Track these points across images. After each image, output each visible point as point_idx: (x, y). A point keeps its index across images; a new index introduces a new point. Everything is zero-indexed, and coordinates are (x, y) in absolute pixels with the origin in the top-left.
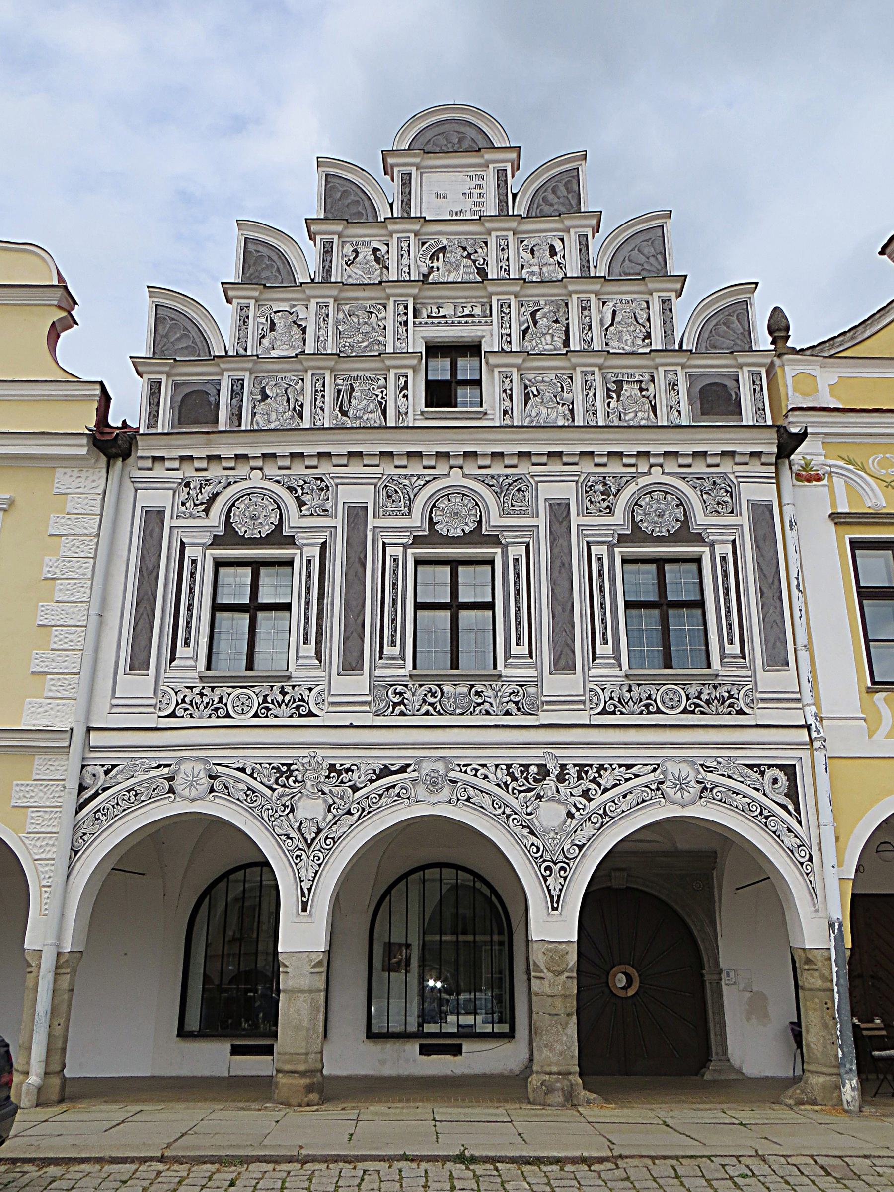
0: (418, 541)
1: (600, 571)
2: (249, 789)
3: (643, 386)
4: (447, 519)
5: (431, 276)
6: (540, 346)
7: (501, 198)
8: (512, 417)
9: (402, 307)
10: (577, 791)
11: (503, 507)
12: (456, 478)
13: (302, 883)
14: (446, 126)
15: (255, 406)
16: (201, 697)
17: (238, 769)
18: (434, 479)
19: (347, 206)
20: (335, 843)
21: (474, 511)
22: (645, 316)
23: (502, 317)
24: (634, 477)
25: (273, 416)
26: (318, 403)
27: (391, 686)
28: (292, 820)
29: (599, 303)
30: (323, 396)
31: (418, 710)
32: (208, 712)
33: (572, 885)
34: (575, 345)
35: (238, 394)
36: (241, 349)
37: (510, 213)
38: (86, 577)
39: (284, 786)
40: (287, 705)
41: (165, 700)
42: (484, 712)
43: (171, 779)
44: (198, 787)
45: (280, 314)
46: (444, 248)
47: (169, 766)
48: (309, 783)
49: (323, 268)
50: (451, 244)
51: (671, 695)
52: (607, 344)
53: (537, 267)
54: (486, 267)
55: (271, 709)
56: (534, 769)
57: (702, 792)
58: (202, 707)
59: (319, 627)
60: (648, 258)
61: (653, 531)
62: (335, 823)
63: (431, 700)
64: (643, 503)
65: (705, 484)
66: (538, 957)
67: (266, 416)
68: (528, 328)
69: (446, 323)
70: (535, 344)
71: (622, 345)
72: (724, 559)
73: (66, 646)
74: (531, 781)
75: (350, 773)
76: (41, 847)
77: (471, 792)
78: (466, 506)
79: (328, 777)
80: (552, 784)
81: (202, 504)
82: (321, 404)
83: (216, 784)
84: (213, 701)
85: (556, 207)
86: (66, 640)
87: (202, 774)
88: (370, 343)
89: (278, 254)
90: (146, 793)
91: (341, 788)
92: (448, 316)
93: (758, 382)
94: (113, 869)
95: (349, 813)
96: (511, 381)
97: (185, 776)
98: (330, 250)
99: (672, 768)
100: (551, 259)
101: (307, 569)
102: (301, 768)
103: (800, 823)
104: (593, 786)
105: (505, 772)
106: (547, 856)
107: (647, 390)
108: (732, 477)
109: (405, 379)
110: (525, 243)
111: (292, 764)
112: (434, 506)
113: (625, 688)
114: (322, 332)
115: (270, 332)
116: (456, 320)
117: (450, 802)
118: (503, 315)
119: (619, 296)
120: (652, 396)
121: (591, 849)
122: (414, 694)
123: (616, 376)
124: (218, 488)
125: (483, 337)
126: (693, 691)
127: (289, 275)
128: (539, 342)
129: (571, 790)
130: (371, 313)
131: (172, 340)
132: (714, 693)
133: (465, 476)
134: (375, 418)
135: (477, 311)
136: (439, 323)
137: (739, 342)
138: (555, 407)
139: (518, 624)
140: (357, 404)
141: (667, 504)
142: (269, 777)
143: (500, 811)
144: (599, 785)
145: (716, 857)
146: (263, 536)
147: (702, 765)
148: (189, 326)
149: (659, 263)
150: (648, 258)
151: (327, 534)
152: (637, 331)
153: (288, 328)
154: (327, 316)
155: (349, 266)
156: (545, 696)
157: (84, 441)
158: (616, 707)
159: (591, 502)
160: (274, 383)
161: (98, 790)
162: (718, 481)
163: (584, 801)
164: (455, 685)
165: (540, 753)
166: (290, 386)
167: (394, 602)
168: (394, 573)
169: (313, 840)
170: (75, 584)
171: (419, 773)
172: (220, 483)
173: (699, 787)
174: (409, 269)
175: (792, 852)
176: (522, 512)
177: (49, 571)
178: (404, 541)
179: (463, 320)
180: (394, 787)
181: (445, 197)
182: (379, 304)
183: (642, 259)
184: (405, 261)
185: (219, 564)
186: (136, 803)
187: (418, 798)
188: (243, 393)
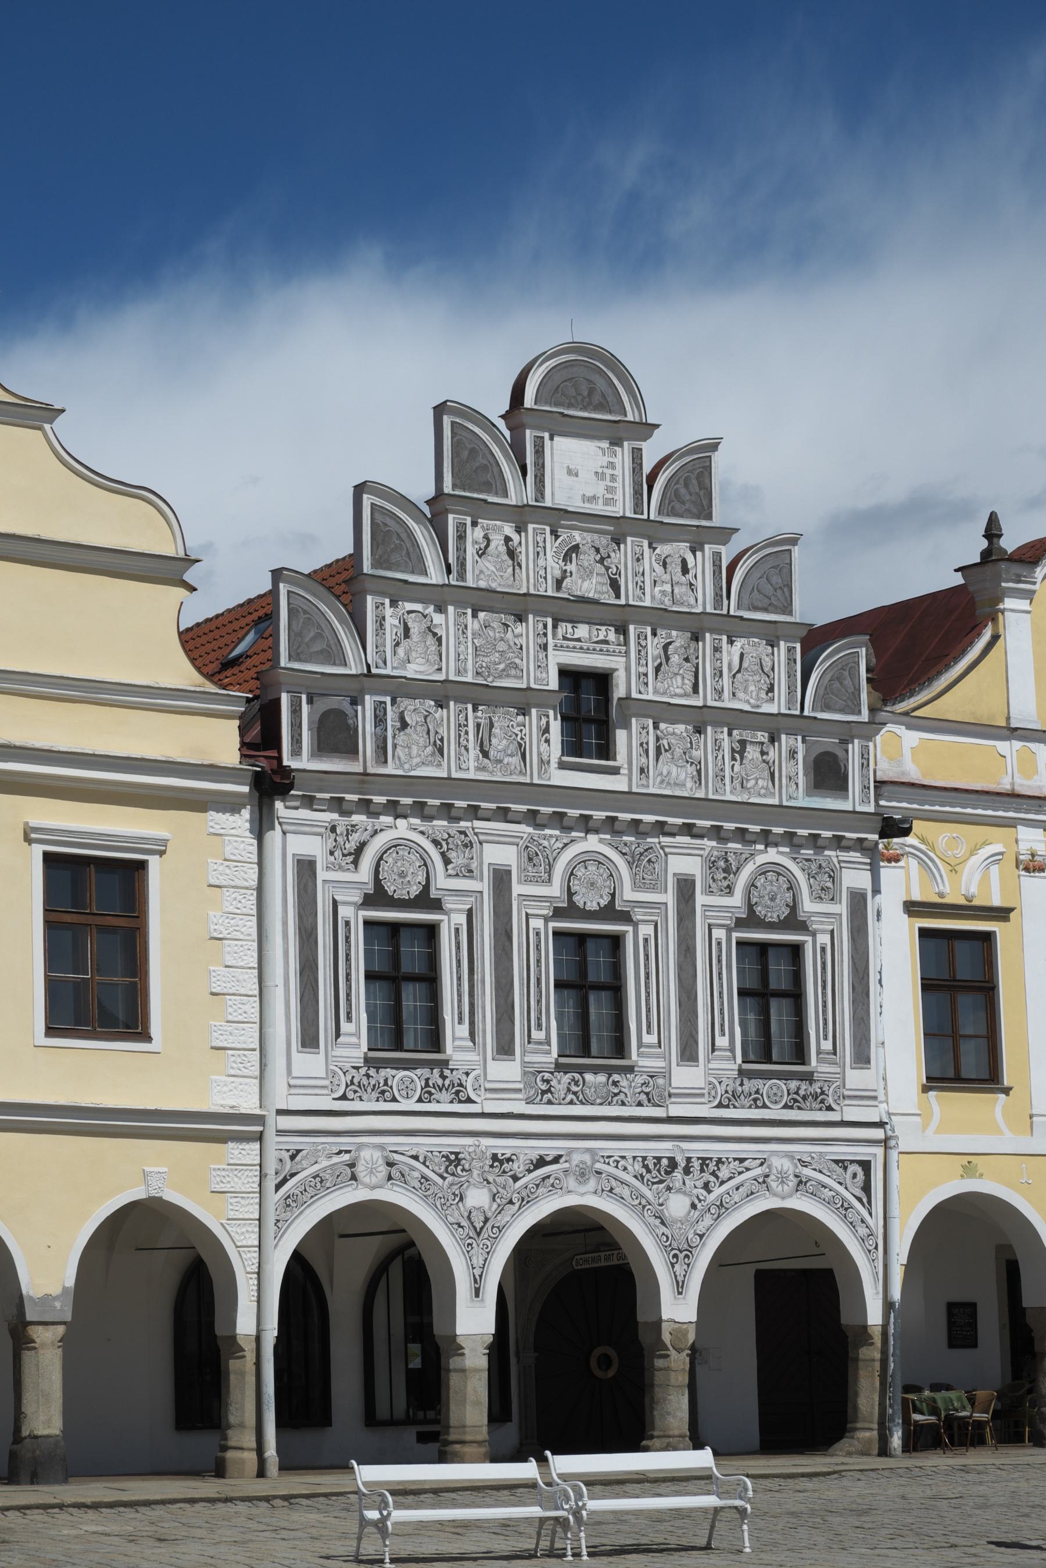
0: (558, 913)
2: (423, 1177)
4: (584, 890)
5: (564, 584)
6: (671, 688)
8: (648, 777)
9: (541, 626)
10: (700, 1184)
13: (475, 1271)
15: (395, 735)
16: (368, 1079)
18: (572, 841)
20: (500, 1231)
21: (608, 882)
22: (770, 664)
23: (640, 651)
24: (752, 855)
25: (415, 750)
27: (540, 1072)
28: (462, 1209)
30: (467, 733)
31: (564, 1099)
32: (375, 1095)
33: (694, 1270)
35: (381, 720)
36: (381, 662)
38: (249, 938)
39: (453, 1174)
40: (447, 1090)
42: (620, 1102)
43: (352, 1165)
44: (378, 1174)
45: (414, 614)
47: (348, 1152)
48: (475, 1172)
49: (458, 558)
50: (584, 542)
52: (734, 694)
53: (669, 586)
54: (619, 579)
55: (433, 1094)
56: (665, 1162)
57: (798, 1185)
58: (369, 1090)
59: (472, 1005)
61: (766, 915)
62: (500, 1213)
63: (574, 1088)
64: (758, 884)
66: (666, 1337)
67: (407, 750)
68: (660, 665)
70: (666, 686)
71: (748, 698)
72: (823, 949)
73: (240, 1018)
74: (662, 1173)
75: (511, 1163)
76: (243, 1233)
77: (614, 1183)
78: (602, 876)
79: (492, 1166)
81: (350, 854)
82: (465, 742)
84: (379, 1083)
85: (687, 506)
86: (240, 1011)
87: (381, 1161)
88: (507, 666)
89: (407, 532)
90: (330, 1179)
91: (504, 1178)
92: (583, 640)
93: (866, 756)
95: (511, 1202)
96: (648, 733)
97: (364, 1163)
98: (463, 534)
99: (777, 1163)
103: (871, 1214)
104: (712, 1179)
105: (641, 1164)
106: (675, 1245)
107: (767, 754)
108: (835, 860)
111: (459, 1153)
112: (572, 874)
113: (738, 1082)
114: (462, 648)
115: (405, 639)
117: (595, 1193)
120: (771, 761)
121: (709, 1239)
124: (365, 836)
125: (617, 670)
127: (420, 562)
130: (507, 626)
131: (306, 640)
136: (574, 648)
137: (850, 704)
139: (648, 1011)
140: (498, 744)
141: (779, 887)
142: (440, 1165)
143: (636, 1202)
144: (717, 1177)
146: (412, 897)
147: (799, 1160)
151: (473, 899)
152: (762, 681)
153: (423, 634)
154: (466, 626)
155: (480, 556)
159: (714, 880)
160: (413, 707)
161: (285, 1176)
162: (824, 865)
163: (705, 1193)
166: (430, 713)
167: (539, 981)
168: (537, 949)
169: (482, 1228)
170: (242, 946)
172: (366, 830)
173: (796, 1181)
174: (546, 573)
175: (863, 1240)
176: (652, 886)
177: (215, 930)
178: (545, 912)
179: (598, 647)
180: (548, 1177)
181: (577, 475)
183: (768, 590)
184: (541, 562)
186: (322, 1190)
187: (570, 1189)
188: (386, 720)
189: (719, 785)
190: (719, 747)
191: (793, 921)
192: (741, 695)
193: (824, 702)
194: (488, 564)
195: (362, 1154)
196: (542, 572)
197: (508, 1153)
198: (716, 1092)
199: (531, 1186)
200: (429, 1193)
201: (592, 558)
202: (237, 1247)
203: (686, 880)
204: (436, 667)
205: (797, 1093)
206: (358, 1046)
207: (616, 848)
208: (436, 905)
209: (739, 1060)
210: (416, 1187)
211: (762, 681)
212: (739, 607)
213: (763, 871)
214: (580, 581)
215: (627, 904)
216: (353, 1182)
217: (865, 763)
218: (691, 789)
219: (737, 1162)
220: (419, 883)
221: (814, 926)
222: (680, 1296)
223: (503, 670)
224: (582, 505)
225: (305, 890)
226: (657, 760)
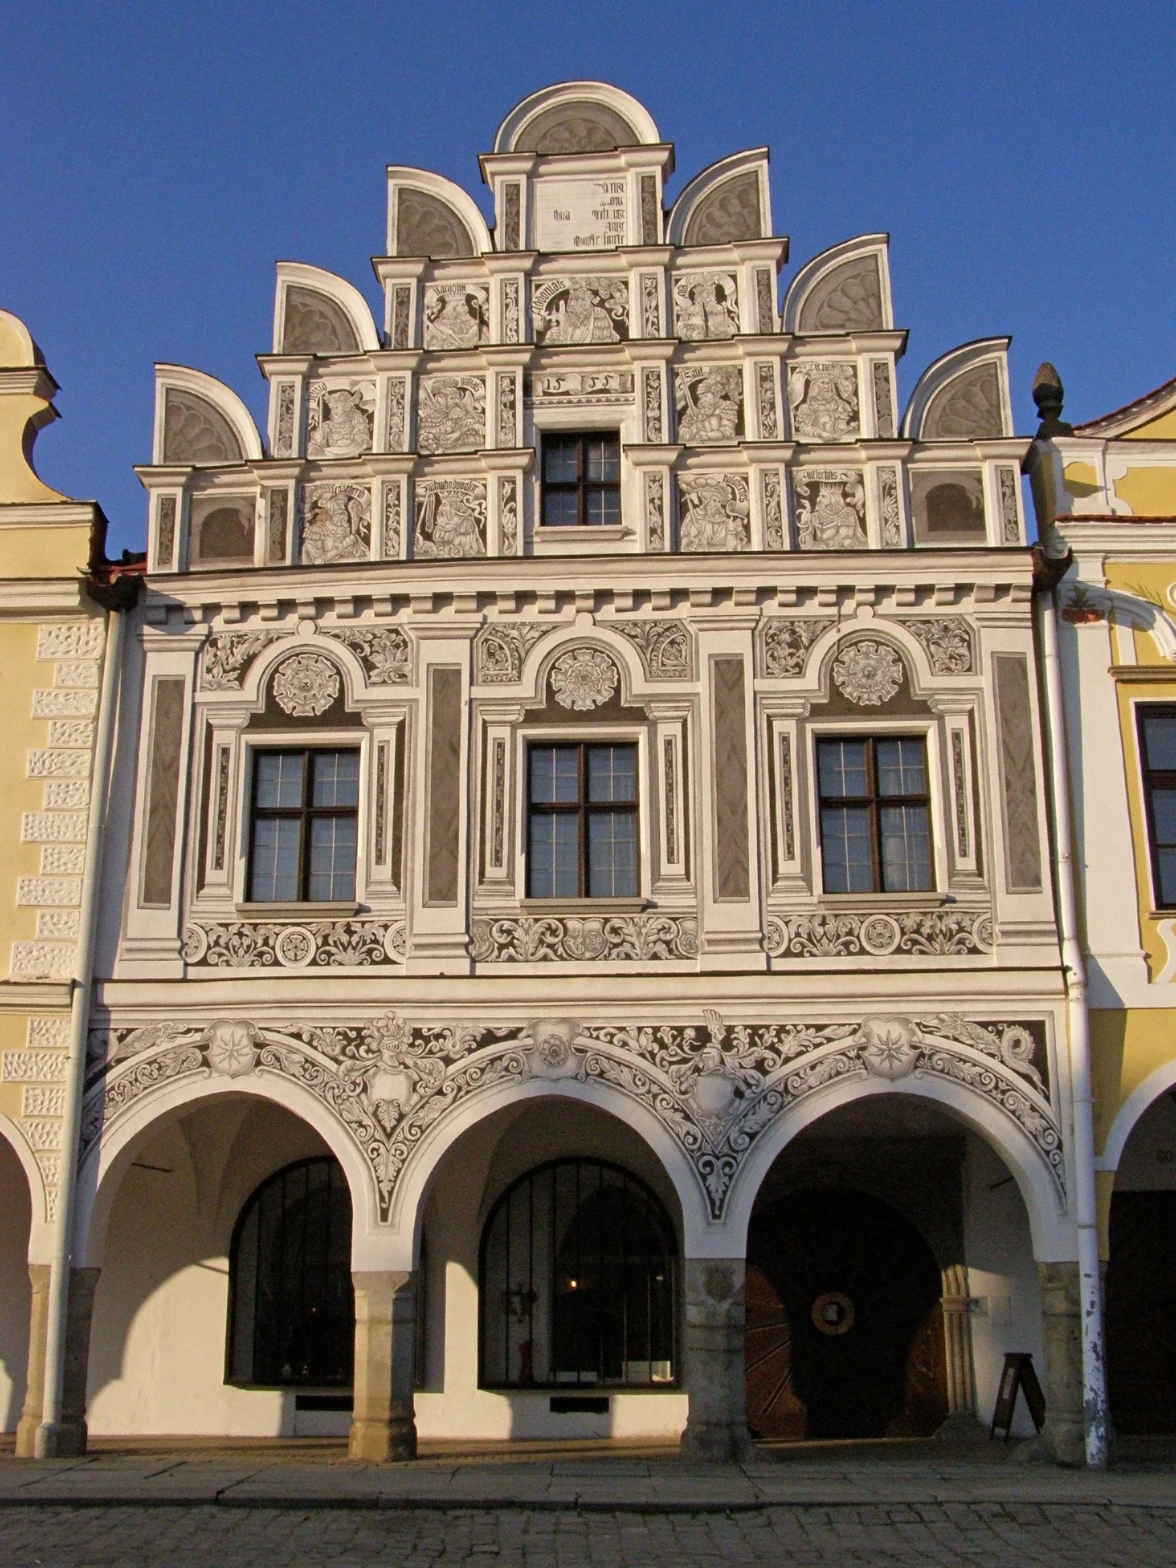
0: (532, 718)
1: (785, 756)
2: (307, 1061)
3: (847, 489)
7: (647, 217)
8: (662, 538)
9: (507, 382)
10: (749, 1062)
11: (650, 666)
12: (584, 627)
14: (569, 112)
18: (554, 628)
19: (429, 235)
20: (422, 1132)
22: (851, 388)
23: (649, 393)
25: (330, 543)
26: (392, 524)
27: (496, 921)
28: (366, 1102)
30: (398, 514)
31: (532, 955)
32: (249, 958)
34: (750, 434)
37: (660, 241)
39: (353, 1057)
40: (354, 948)
42: (623, 955)
43: (204, 1048)
44: (241, 1059)
48: (386, 1054)
49: (397, 326)
50: (577, 286)
56: (690, 1033)
57: (918, 1059)
58: (241, 952)
60: (855, 303)
61: (859, 698)
62: (422, 1107)
63: (550, 939)
64: (846, 659)
65: (933, 630)
69: (570, 402)
70: (695, 431)
71: (819, 431)
72: (957, 736)
74: (686, 1049)
75: (441, 1040)
77: (605, 1064)
79: (412, 1045)
80: (714, 1052)
81: (234, 669)
85: (726, 228)
87: (245, 1041)
88: (462, 434)
89: (333, 308)
91: (430, 1060)
93: (1009, 483)
94: (134, 1164)
95: (440, 1092)
96: (661, 486)
99: (879, 1029)
100: (719, 307)
102: (376, 1034)
103: (1047, 1098)
104: (769, 1054)
105: (651, 1037)
106: (707, 1148)
107: (853, 495)
108: (970, 620)
109: (512, 486)
110: (680, 283)
112: (553, 667)
113: (817, 921)
114: (396, 420)
116: (583, 398)
117: (576, 1078)
119: (815, 359)
120: (860, 503)
122: (527, 932)
123: (809, 475)
124: (256, 647)
125: (621, 421)
126: (910, 923)
130: (465, 390)
132: (939, 925)
134: (469, 543)
135: (614, 384)
137: (983, 423)
138: (723, 522)
139: (670, 832)
140: (446, 522)
142: (333, 1046)
147: (918, 1024)
148: (214, 418)
149: (872, 310)
150: (855, 303)
152: (840, 409)
153: (349, 416)
154: (403, 397)
155: (432, 321)
156: (707, 933)
157: (75, 587)
158: (803, 946)
162: (952, 626)
163: (757, 1074)
164: (583, 919)
165: (697, 1011)
167: (499, 805)
169: (394, 1128)
171: (535, 1040)
173: (913, 1053)
175: (1035, 1137)
176: (677, 674)
178: (512, 718)
180: (500, 1058)
181: (568, 218)
183: (847, 304)
185: (258, 754)
189: (771, 537)
190: (772, 493)
192: (808, 429)
194: (443, 328)
195: (219, 1032)
196: (513, 325)
197: (437, 1027)
199: (472, 1070)
200: (314, 1082)
203: (729, 662)
204: (365, 446)
205: (917, 931)
206: (229, 898)
207: (622, 631)
210: (297, 1074)
211: (840, 409)
214: (570, 329)
216: (205, 1069)
217: (1008, 492)
219: (812, 1030)
220: (329, 695)
221: (941, 707)
222: (717, 1221)
223: (457, 439)
225: (167, 713)
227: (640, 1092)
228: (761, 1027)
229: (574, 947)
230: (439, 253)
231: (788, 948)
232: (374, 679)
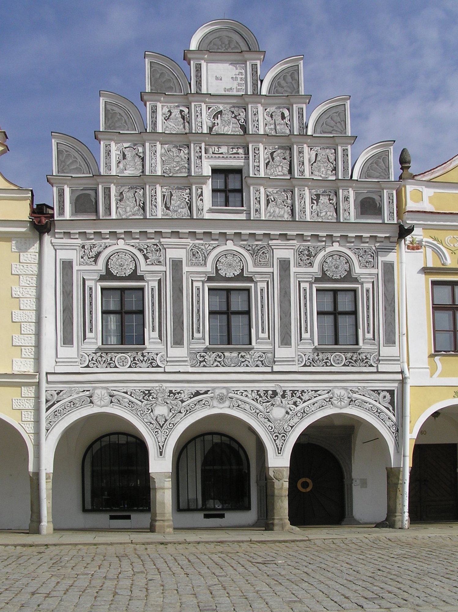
0: (210, 279)
1: (305, 296)
2: (130, 401)
8: (260, 213)
9: (198, 148)
17: (124, 392)
18: (218, 246)
23: (255, 156)
27: (198, 353)
28: (152, 415)
29: (308, 149)
39: (147, 400)
40: (145, 362)
41: (83, 359)
42: (245, 365)
43: (90, 397)
44: (105, 400)
46: (221, 111)
48: (160, 399)
50: (225, 109)
51: (338, 357)
52: (312, 173)
58: (102, 363)
63: (220, 360)
64: (328, 261)
68: (269, 162)
70: (272, 171)
71: (320, 174)
74: (269, 398)
75: (180, 394)
77: (240, 403)
79: (169, 396)
83: (113, 399)
85: (285, 89)
87: (106, 395)
88: (180, 168)
90: (79, 403)
95: (180, 412)
96: (260, 193)
99: (337, 392)
101: (152, 293)
104: (299, 400)
106: (276, 431)
109: (201, 190)
112: (218, 260)
113: (316, 354)
118: (255, 154)
122: (210, 357)
128: (275, 170)
129: (288, 402)
130: (181, 150)
133: (235, 245)
141: (340, 262)
142: (139, 396)
144: (302, 399)
145: (354, 429)
151: (161, 275)
158: (311, 363)
159: (301, 260)
163: (294, 406)
165: (273, 385)
167: (198, 311)
168: (198, 296)
169: (163, 425)
174: (202, 124)
178: (203, 279)
180: (202, 400)
181: (221, 79)
182: (185, 145)
184: (199, 119)
186: (74, 408)
187: (214, 405)
190: (302, 198)
191: (349, 277)
193: (367, 171)
196: (200, 124)
198: (302, 360)
199: (191, 405)
200: (133, 408)
201: (230, 115)
202: (27, 433)
203: (284, 261)
207: (244, 248)
208: (141, 278)
209: (316, 344)
210: (126, 406)
212: (315, 132)
213: (331, 255)
215: (250, 273)
218: (288, 218)
224: (224, 93)
226: (267, 206)
227: (252, 412)
228: (295, 390)
229: (227, 363)
230: (168, 91)
231: (305, 363)
232: (148, 263)
